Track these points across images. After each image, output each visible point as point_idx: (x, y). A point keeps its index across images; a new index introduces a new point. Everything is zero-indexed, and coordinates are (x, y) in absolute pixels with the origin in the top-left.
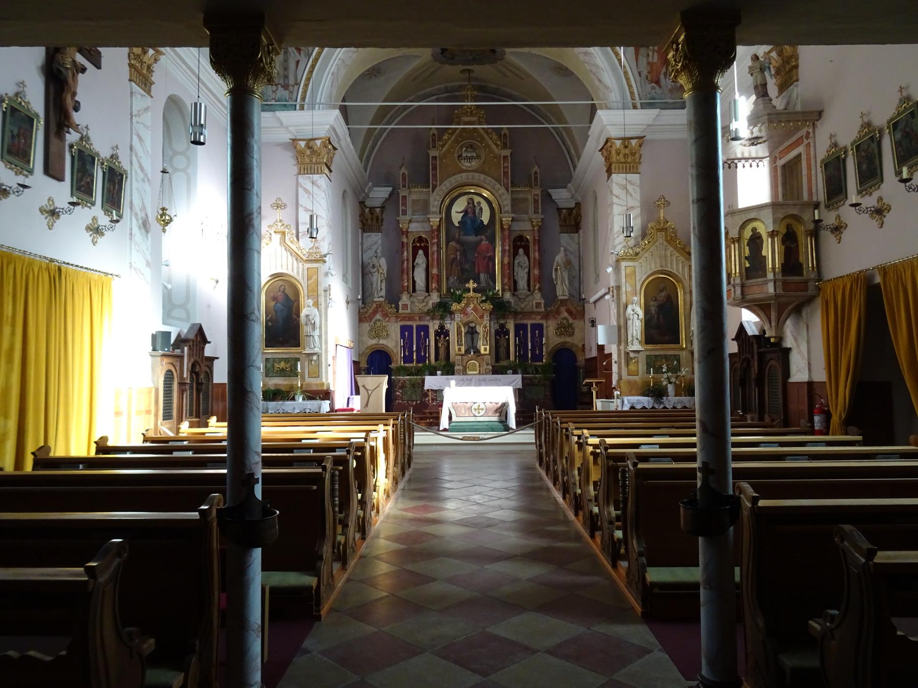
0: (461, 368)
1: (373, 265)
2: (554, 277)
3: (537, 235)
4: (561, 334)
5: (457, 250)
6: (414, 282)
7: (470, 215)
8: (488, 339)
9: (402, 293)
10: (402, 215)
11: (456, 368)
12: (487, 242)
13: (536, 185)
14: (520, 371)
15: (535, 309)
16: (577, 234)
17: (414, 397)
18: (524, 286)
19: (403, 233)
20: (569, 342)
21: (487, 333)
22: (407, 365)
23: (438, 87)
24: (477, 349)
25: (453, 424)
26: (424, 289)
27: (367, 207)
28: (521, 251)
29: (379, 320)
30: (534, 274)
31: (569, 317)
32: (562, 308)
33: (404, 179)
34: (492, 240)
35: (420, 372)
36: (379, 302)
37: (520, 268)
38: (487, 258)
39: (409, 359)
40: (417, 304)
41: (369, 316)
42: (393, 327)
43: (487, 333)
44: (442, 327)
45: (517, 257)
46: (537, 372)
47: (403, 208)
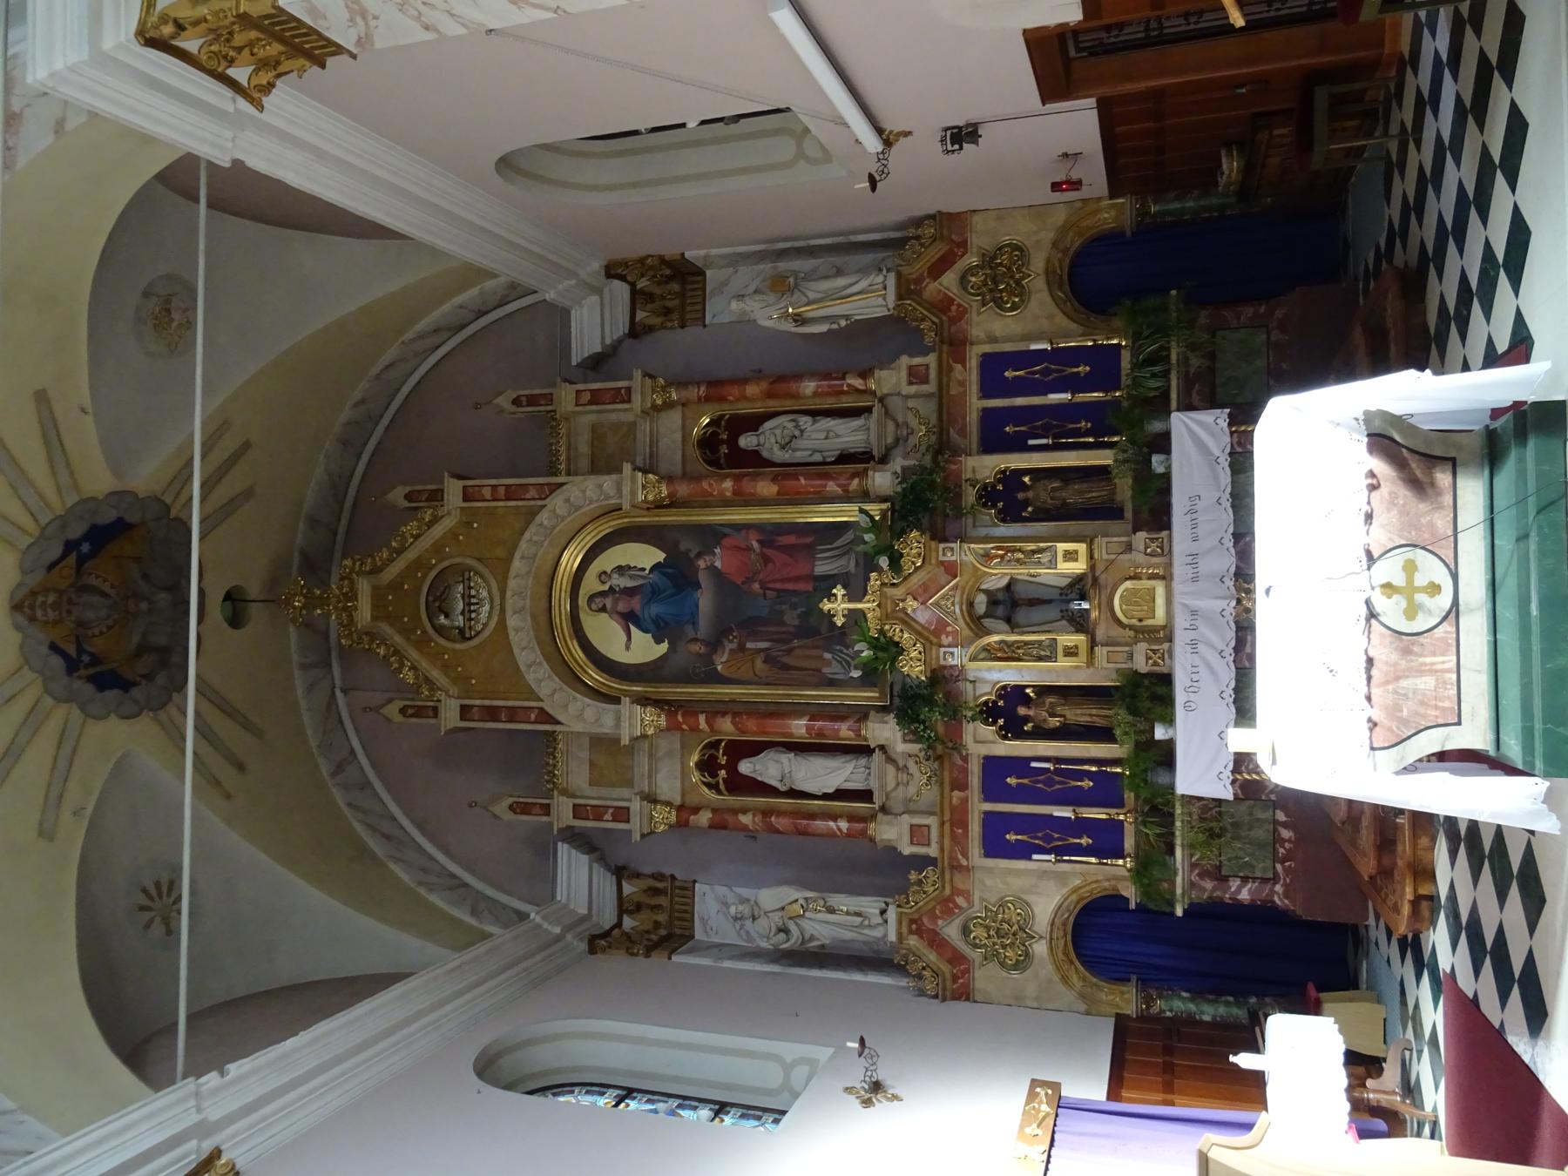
0: (1141, 649)
1: (780, 930)
2: (822, 328)
3: (693, 393)
4: (1020, 290)
5: (742, 648)
6: (841, 794)
7: (636, 604)
8: (1032, 546)
9: (872, 840)
10: (628, 821)
11: (1141, 665)
12: (718, 551)
13: (549, 399)
14: (1157, 426)
15: (931, 388)
16: (709, 273)
17: (1260, 833)
18: (858, 429)
19: (682, 824)
20: (1048, 261)
21: (1008, 550)
22: (1129, 843)
23: (299, 692)
24: (1071, 585)
25: (1513, 750)
26: (863, 761)
27: (619, 925)
28: (746, 441)
29: (966, 931)
30: (816, 394)
31: (961, 265)
32: (926, 294)
33: (525, 809)
34: (711, 536)
35: (1159, 807)
36: (900, 923)
37: (797, 443)
38: (768, 552)
39: (1106, 843)
40: (912, 790)
41: (950, 962)
42: (989, 882)
43: (1008, 550)
44: (989, 713)
45: (765, 454)
46: (1159, 358)
47: (608, 817)
